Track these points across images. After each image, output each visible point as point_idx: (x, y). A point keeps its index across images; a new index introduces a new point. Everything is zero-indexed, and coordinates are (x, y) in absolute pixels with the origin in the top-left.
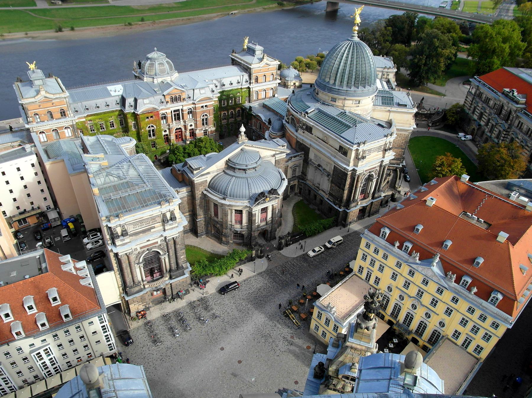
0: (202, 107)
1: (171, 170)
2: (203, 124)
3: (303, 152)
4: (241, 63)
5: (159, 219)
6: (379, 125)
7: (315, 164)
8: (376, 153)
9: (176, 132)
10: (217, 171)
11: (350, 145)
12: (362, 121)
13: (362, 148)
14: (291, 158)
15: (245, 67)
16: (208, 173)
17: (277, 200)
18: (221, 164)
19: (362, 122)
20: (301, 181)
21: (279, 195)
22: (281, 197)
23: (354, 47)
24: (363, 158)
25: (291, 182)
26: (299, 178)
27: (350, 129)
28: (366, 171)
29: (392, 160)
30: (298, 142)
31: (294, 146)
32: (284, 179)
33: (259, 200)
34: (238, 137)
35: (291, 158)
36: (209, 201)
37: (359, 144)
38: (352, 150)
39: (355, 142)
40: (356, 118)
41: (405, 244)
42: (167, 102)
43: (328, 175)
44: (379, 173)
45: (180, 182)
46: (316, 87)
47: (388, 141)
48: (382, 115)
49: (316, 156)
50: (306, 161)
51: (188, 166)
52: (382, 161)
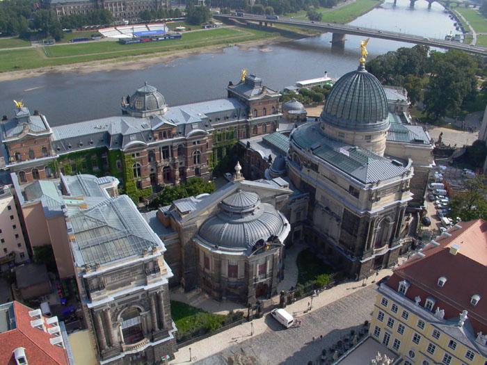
0: (194, 143)
1: (157, 213)
3: (308, 193)
5: (139, 271)
7: (321, 206)
9: (164, 171)
20: (306, 226)
24: (377, 200)
26: (304, 222)
28: (381, 214)
30: (302, 182)
31: (298, 185)
39: (367, 181)
41: (427, 300)
43: (338, 220)
45: (167, 228)
49: (323, 197)
50: (313, 203)
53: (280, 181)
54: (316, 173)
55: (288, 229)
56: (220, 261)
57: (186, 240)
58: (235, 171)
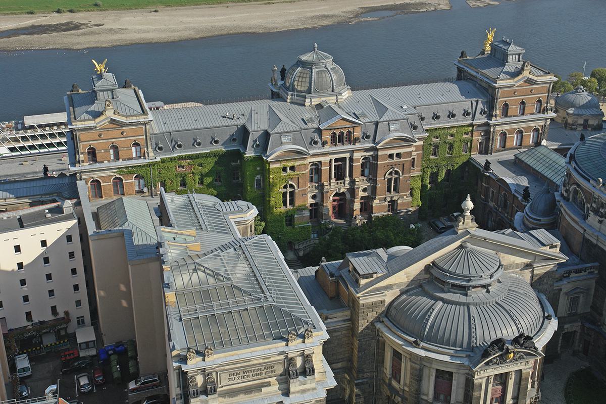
0: (391, 156)
1: (317, 272)
2: (389, 190)
4: (476, 77)
9: (334, 201)
14: (570, 272)
15: (484, 85)
16: (389, 287)
17: (532, 361)
20: (587, 325)
25: (566, 326)
30: (586, 241)
31: (577, 247)
32: (549, 318)
33: (490, 355)
35: (570, 272)
42: (324, 144)
45: (331, 298)
51: (351, 268)
53: (542, 234)
55: (553, 325)
56: (421, 370)
57: (363, 324)
58: (462, 211)
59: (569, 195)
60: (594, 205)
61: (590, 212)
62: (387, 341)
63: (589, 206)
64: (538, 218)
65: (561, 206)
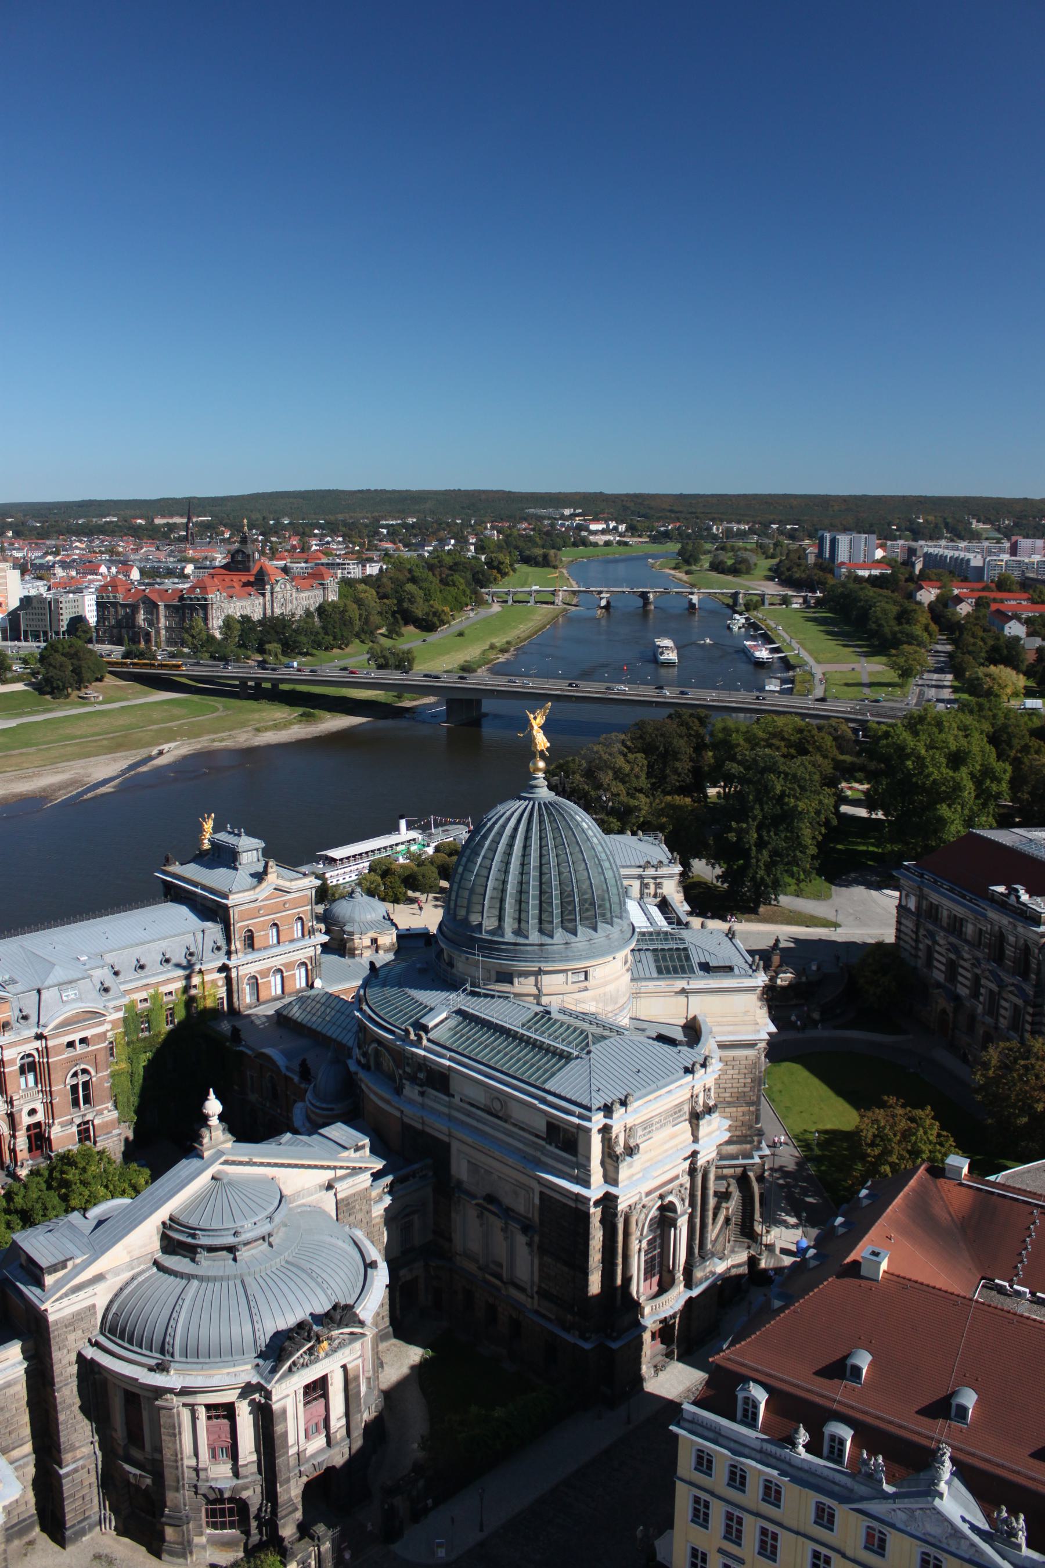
0: (71, 1044)
6: (661, 1038)
7: (473, 1196)
8: (669, 1130)
10: (130, 1266)
11: (580, 1117)
12: (606, 1033)
13: (619, 1121)
15: (209, 904)
16: (99, 1278)
17: (357, 1345)
18: (144, 1238)
19: (604, 1038)
21: (362, 1323)
22: (370, 1332)
23: (541, 815)
24: (631, 1151)
27: (573, 1063)
28: (648, 1194)
29: (729, 1142)
30: (407, 1128)
32: (373, 1265)
33: (291, 1354)
34: (198, 1138)
36: (105, 1383)
37: (608, 1110)
38: (588, 1131)
40: (585, 1026)
43: (526, 1229)
44: (692, 1196)
46: (443, 946)
47: (698, 1089)
48: (665, 1005)
51: (23, 1260)
52: (694, 1154)
54: (447, 1098)
55: (381, 1277)
59: (368, 1061)
60: (408, 1070)
61: (404, 1081)
62: (109, 1377)
63: (401, 1072)
64: (330, 1106)
65: (361, 1080)
